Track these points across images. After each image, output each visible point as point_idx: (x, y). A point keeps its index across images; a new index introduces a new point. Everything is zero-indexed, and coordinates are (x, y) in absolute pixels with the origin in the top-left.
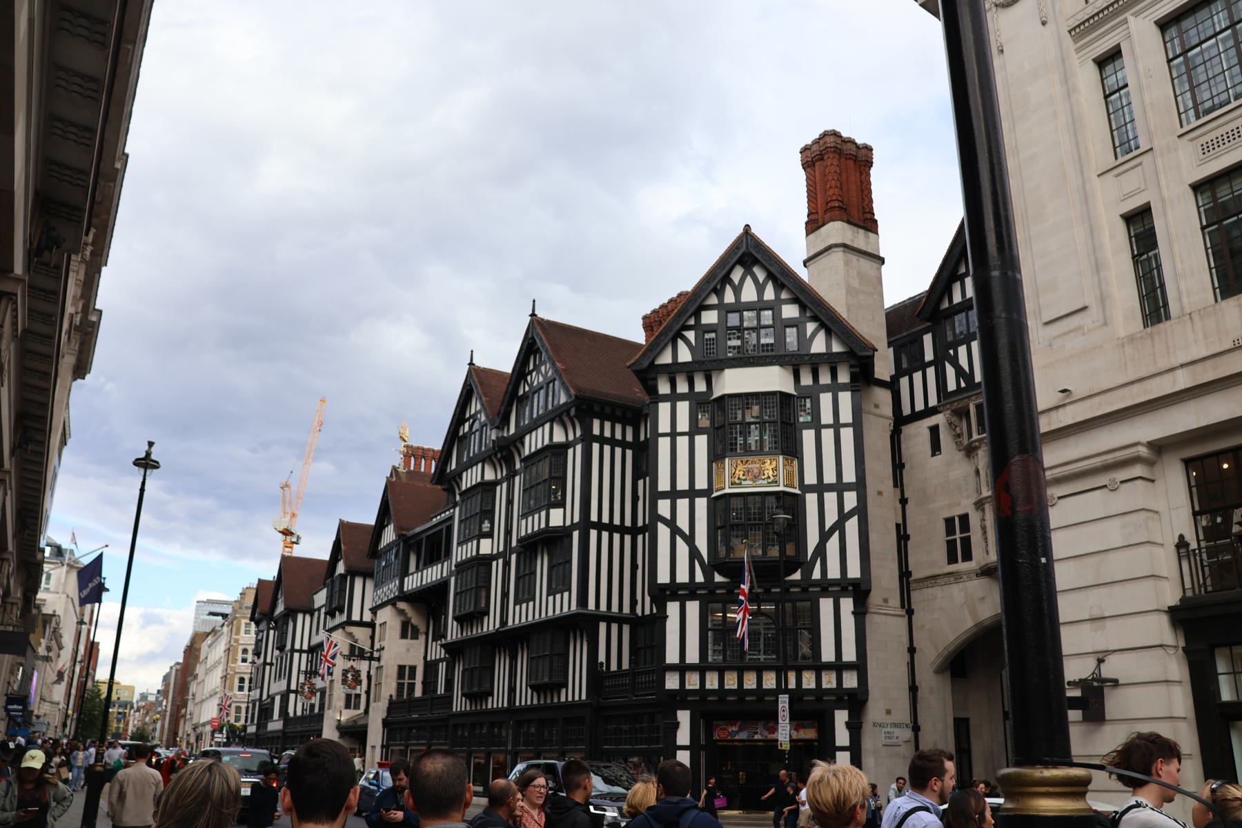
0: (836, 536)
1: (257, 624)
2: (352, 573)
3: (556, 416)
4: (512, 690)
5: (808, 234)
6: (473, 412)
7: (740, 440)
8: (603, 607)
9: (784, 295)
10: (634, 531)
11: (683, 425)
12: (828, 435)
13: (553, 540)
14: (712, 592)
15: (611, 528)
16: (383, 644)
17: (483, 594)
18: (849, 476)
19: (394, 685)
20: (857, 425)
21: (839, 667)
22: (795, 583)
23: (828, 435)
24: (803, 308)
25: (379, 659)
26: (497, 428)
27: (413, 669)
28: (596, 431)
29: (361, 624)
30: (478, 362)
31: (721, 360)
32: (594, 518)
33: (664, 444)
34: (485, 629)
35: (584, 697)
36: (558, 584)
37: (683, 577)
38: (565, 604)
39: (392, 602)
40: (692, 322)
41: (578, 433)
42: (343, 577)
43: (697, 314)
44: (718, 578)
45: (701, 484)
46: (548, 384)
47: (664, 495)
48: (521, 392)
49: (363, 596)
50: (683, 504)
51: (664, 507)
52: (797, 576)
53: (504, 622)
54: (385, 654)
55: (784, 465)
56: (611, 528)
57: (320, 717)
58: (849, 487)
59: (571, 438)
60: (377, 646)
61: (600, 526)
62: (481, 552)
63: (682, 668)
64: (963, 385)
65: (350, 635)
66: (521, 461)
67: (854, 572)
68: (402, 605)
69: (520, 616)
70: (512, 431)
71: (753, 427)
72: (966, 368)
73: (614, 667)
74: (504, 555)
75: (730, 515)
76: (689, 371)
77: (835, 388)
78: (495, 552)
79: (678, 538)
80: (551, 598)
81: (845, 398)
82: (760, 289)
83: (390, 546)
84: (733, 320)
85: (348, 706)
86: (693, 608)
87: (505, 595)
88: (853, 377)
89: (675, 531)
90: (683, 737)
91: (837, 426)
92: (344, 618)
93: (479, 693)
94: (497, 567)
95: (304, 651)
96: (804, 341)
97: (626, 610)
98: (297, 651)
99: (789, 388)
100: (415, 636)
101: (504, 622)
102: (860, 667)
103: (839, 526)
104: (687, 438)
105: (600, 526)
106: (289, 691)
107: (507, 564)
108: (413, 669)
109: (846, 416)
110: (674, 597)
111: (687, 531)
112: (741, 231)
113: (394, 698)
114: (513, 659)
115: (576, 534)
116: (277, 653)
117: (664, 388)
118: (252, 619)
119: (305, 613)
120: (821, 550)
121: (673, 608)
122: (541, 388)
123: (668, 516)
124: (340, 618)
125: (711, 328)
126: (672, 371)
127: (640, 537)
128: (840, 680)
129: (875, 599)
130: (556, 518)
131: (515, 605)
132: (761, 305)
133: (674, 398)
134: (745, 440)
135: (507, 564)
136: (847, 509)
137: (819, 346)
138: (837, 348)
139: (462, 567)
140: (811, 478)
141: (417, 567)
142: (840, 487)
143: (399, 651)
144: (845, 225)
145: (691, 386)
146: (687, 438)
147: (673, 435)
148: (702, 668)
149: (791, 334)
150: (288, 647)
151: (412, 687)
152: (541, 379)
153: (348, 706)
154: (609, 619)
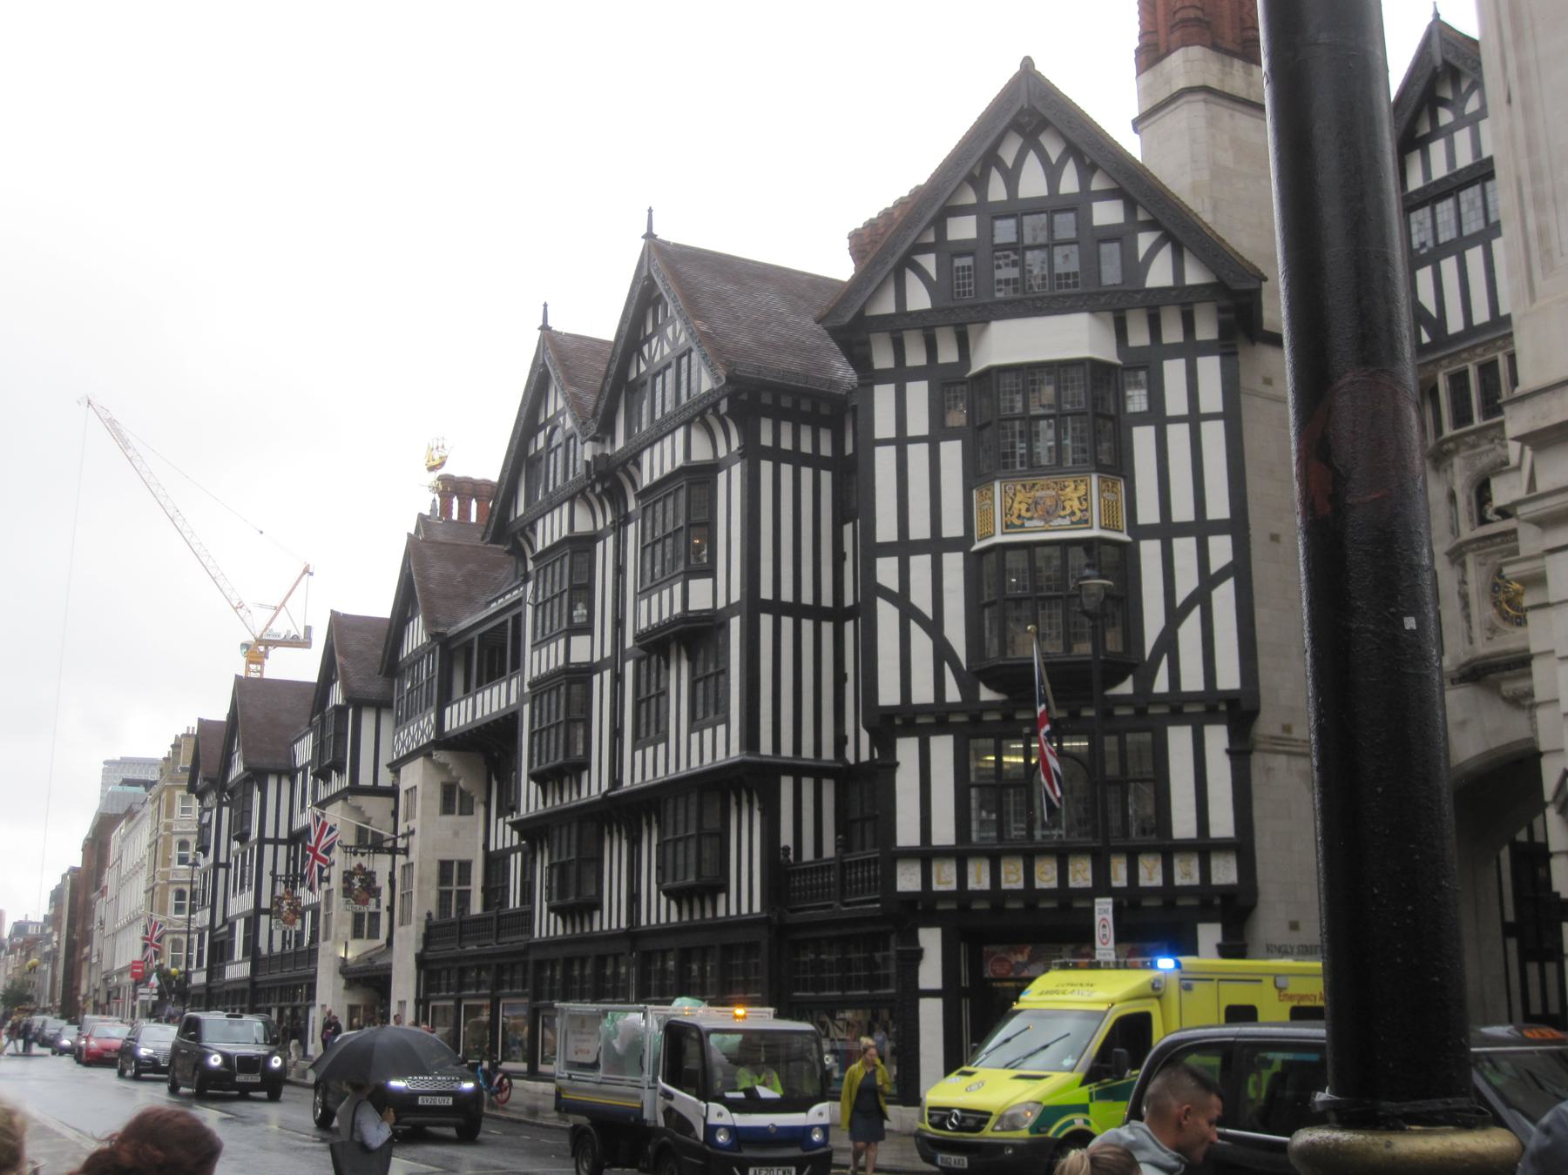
0: (1196, 614)
1: (201, 796)
2: (357, 703)
3: (698, 415)
4: (634, 898)
5: (1138, 74)
6: (551, 412)
7: (1021, 448)
8: (787, 750)
9: (1097, 184)
10: (838, 615)
11: (919, 423)
12: (1178, 436)
13: (694, 636)
14: (976, 720)
15: (797, 610)
16: (415, 824)
17: (580, 732)
18: (1218, 507)
19: (433, 895)
20: (1232, 416)
21: (1204, 847)
22: (1122, 700)
23: (1178, 436)
24: (1131, 206)
25: (406, 851)
26: (594, 439)
27: (465, 866)
28: (766, 439)
29: (375, 791)
30: (557, 325)
31: (985, 305)
32: (766, 593)
33: (885, 459)
34: (584, 794)
35: (757, 908)
36: (706, 710)
37: (923, 693)
38: (720, 746)
39: (423, 752)
40: (930, 238)
41: (735, 444)
42: (340, 711)
43: (939, 223)
44: (986, 694)
45: (953, 527)
46: (679, 358)
47: (887, 549)
48: (633, 375)
49: (380, 743)
50: (920, 565)
51: (887, 571)
52: (1126, 688)
53: (616, 781)
54: (415, 842)
55: (1100, 492)
56: (797, 610)
57: (311, 955)
58: (1219, 527)
59: (722, 452)
60: (402, 829)
61: (777, 608)
62: (573, 659)
63: (926, 855)
64: (1426, 339)
65: (358, 810)
66: (639, 496)
67: (1229, 678)
68: (440, 756)
69: (644, 768)
70: (620, 443)
71: (1043, 424)
72: (1431, 307)
73: (808, 854)
74: (614, 664)
75: (1005, 584)
76: (926, 325)
77: (1190, 350)
78: (597, 658)
79: (914, 626)
80: (695, 737)
81: (1210, 369)
82: (1053, 173)
83: (418, 656)
84: (1005, 231)
85: (357, 933)
86: (943, 748)
87: (617, 733)
88: (1226, 331)
89: (908, 612)
90: (930, 974)
91: (1195, 418)
92: (346, 781)
93: (577, 907)
94: (601, 684)
95: (282, 842)
96: (1135, 268)
97: (828, 753)
98: (270, 841)
99: (1107, 352)
100: (467, 810)
101: (616, 781)
102: (1242, 846)
103: (1201, 598)
104: (924, 447)
105: (777, 608)
106: (258, 910)
107: (618, 678)
108: (465, 866)
109: (1211, 399)
110: (909, 729)
111: (927, 610)
112: (1017, 68)
113: (434, 915)
114: (635, 844)
115: (735, 624)
116: (236, 845)
117: (883, 359)
118: (191, 788)
119: (280, 774)
120: (1168, 642)
121: (907, 750)
122: (668, 366)
124: (339, 783)
125: (964, 249)
126: (899, 325)
127: (849, 627)
128: (1205, 872)
129: (1267, 725)
130: (701, 595)
131: (634, 750)
133: (900, 376)
134: (1030, 448)
135: (618, 678)
136: (1215, 565)
137: (1160, 275)
138: (1194, 275)
139: (541, 687)
140: (1148, 513)
141: (467, 690)
142: (1202, 529)
143: (438, 834)
144: (1209, 52)
145: (932, 351)
146: (924, 447)
147: (901, 441)
148: (960, 855)
149: (1110, 252)
150: (254, 835)
151: (464, 897)
152: (667, 350)
153: (357, 933)
154: (798, 771)
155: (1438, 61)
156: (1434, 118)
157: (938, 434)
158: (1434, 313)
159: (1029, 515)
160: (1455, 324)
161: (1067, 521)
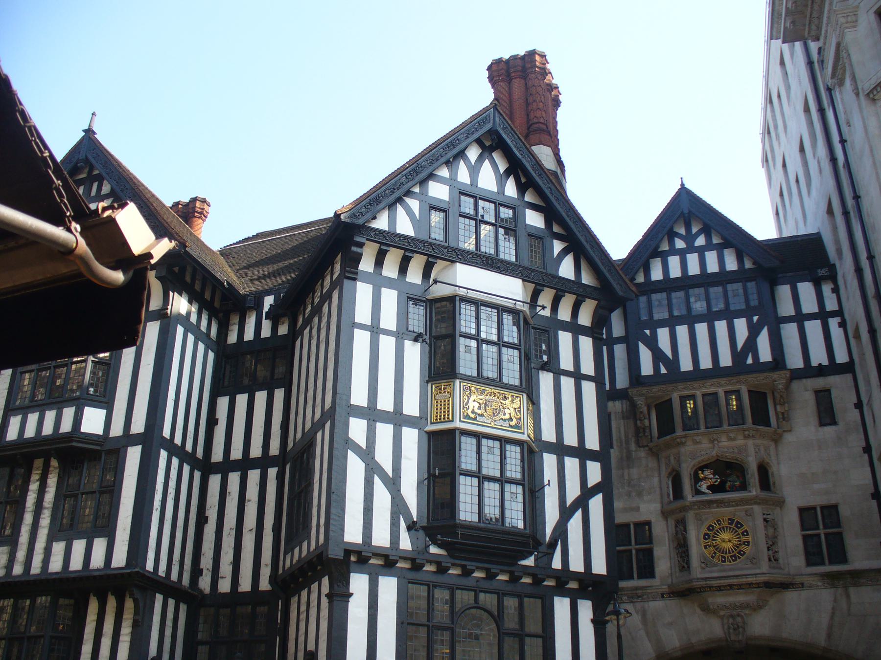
10: (205, 467)
18: (593, 442)
22: (526, 570)
33: (361, 340)
37: (381, 538)
45: (411, 408)
50: (385, 431)
51: (357, 429)
64: (663, 370)
72: (669, 353)
79: (377, 479)
81: (586, 344)
89: (372, 469)
111: (389, 471)
117: (366, 265)
120: (561, 531)
123: (362, 443)
127: (215, 481)
130: (93, 421)
132: (500, 199)
142: (582, 453)
155: (686, 211)
156: (671, 243)
157: (401, 334)
158: (670, 356)
159: (479, 412)
160: (686, 365)
161: (506, 424)
